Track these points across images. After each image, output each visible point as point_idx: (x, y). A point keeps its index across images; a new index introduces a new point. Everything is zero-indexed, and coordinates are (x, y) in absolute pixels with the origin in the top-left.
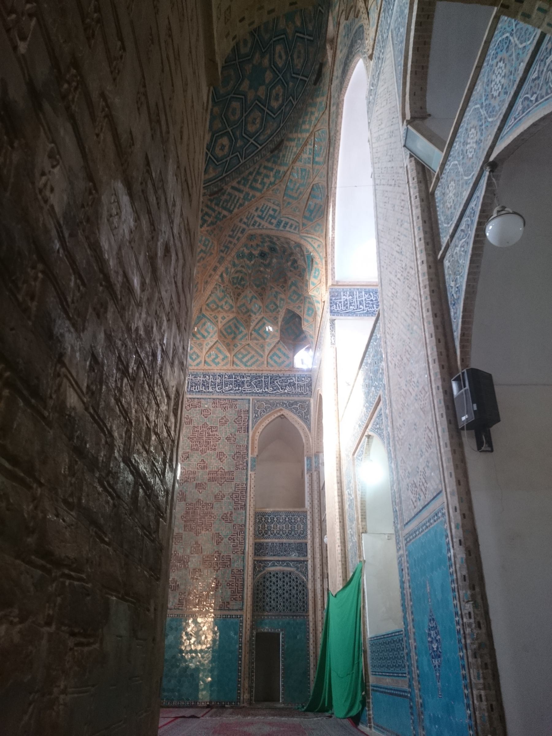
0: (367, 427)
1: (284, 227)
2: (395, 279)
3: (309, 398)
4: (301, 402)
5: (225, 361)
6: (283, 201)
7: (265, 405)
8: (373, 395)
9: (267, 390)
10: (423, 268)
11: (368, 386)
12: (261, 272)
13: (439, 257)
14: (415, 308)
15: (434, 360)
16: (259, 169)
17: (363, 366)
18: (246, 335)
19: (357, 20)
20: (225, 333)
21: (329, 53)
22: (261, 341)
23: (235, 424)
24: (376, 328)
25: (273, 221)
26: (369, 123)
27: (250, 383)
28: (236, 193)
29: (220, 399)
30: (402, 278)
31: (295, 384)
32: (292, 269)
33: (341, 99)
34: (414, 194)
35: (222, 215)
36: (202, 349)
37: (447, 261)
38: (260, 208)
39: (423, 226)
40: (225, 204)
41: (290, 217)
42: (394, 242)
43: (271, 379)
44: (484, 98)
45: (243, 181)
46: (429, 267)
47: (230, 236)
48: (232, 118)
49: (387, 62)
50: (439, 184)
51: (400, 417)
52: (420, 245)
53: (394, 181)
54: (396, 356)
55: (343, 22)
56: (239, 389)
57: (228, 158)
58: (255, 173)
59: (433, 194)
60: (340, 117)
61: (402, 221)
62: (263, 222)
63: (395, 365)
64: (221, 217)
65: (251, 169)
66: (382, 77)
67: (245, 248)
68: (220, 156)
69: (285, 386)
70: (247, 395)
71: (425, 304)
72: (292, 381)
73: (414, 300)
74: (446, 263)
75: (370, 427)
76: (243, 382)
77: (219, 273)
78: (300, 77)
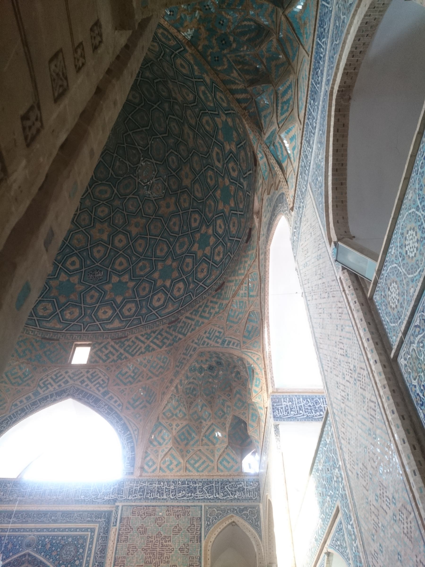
0: (325, 542)
1: (228, 344)
2: (344, 382)
3: (258, 504)
4: (251, 508)
5: (179, 467)
6: (226, 325)
7: (216, 512)
8: (329, 505)
9: (218, 496)
10: (377, 368)
11: (321, 495)
12: (210, 383)
13: (392, 355)
14: (375, 411)
15: (414, 472)
16: (207, 303)
17: (313, 473)
18: (197, 441)
19: (277, 191)
20: (178, 439)
21: (256, 221)
22: (212, 446)
23: (188, 533)
24: (324, 433)
25: (219, 340)
26: (295, 256)
27: (202, 489)
28: (189, 321)
29: (173, 506)
30: (352, 381)
31: (244, 489)
32: (236, 379)
33: (267, 249)
34: (352, 300)
35: (178, 338)
36: (158, 456)
37: (403, 359)
38: (208, 331)
39: (368, 327)
40: (181, 329)
41: (233, 337)
42: (336, 346)
43: (221, 484)
44: (419, 202)
45: (194, 313)
46: (384, 366)
47: (184, 354)
48: (186, 269)
49: (308, 206)
50: (377, 289)
51: (374, 540)
52: (369, 345)
53: (327, 294)
54: (358, 464)
55: (266, 197)
56: (191, 496)
57: (183, 297)
58: (203, 306)
59: (371, 298)
60: (267, 261)
61: (342, 326)
62: (210, 342)
63: (358, 474)
64: (177, 339)
66: (303, 219)
67: (196, 363)
68: (177, 296)
69: (235, 492)
70: (199, 502)
71: (388, 405)
72: (241, 486)
73: (372, 402)
74: (402, 361)
75: (328, 542)
76: (195, 488)
77: (175, 385)
78: (235, 239)
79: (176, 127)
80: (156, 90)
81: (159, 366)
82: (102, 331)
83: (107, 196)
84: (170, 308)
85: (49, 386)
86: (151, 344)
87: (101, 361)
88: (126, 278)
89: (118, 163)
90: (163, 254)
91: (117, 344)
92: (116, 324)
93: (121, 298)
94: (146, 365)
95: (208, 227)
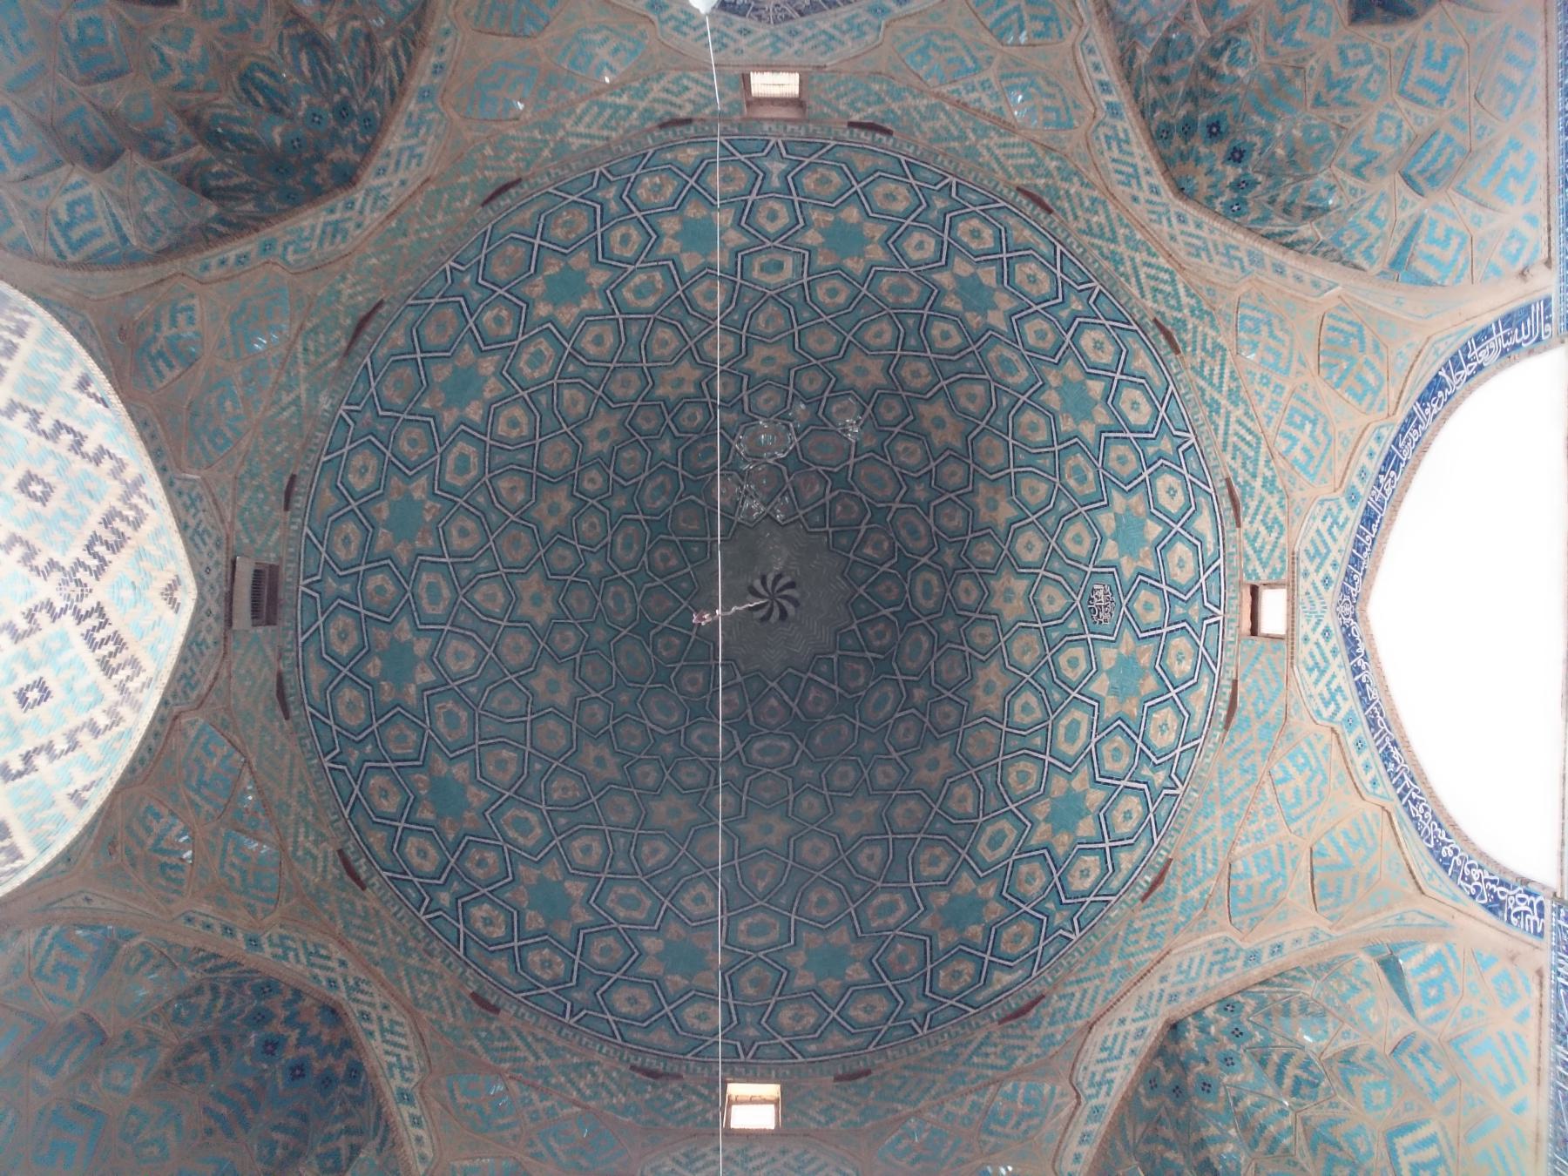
28: (1143, 276)
62: (1141, 165)
65: (1096, 252)
67: (1217, 202)
79: (764, 397)
80: (696, 437)
81: (1273, 343)
82: (1221, 561)
83: (935, 580)
84: (1142, 362)
85: (1333, 686)
86: (1225, 388)
87: (1283, 540)
88: (1106, 520)
89: (868, 551)
90: (1042, 421)
91: (1247, 508)
92: (1203, 524)
93: (1149, 522)
94: (1277, 386)
95: (942, 292)
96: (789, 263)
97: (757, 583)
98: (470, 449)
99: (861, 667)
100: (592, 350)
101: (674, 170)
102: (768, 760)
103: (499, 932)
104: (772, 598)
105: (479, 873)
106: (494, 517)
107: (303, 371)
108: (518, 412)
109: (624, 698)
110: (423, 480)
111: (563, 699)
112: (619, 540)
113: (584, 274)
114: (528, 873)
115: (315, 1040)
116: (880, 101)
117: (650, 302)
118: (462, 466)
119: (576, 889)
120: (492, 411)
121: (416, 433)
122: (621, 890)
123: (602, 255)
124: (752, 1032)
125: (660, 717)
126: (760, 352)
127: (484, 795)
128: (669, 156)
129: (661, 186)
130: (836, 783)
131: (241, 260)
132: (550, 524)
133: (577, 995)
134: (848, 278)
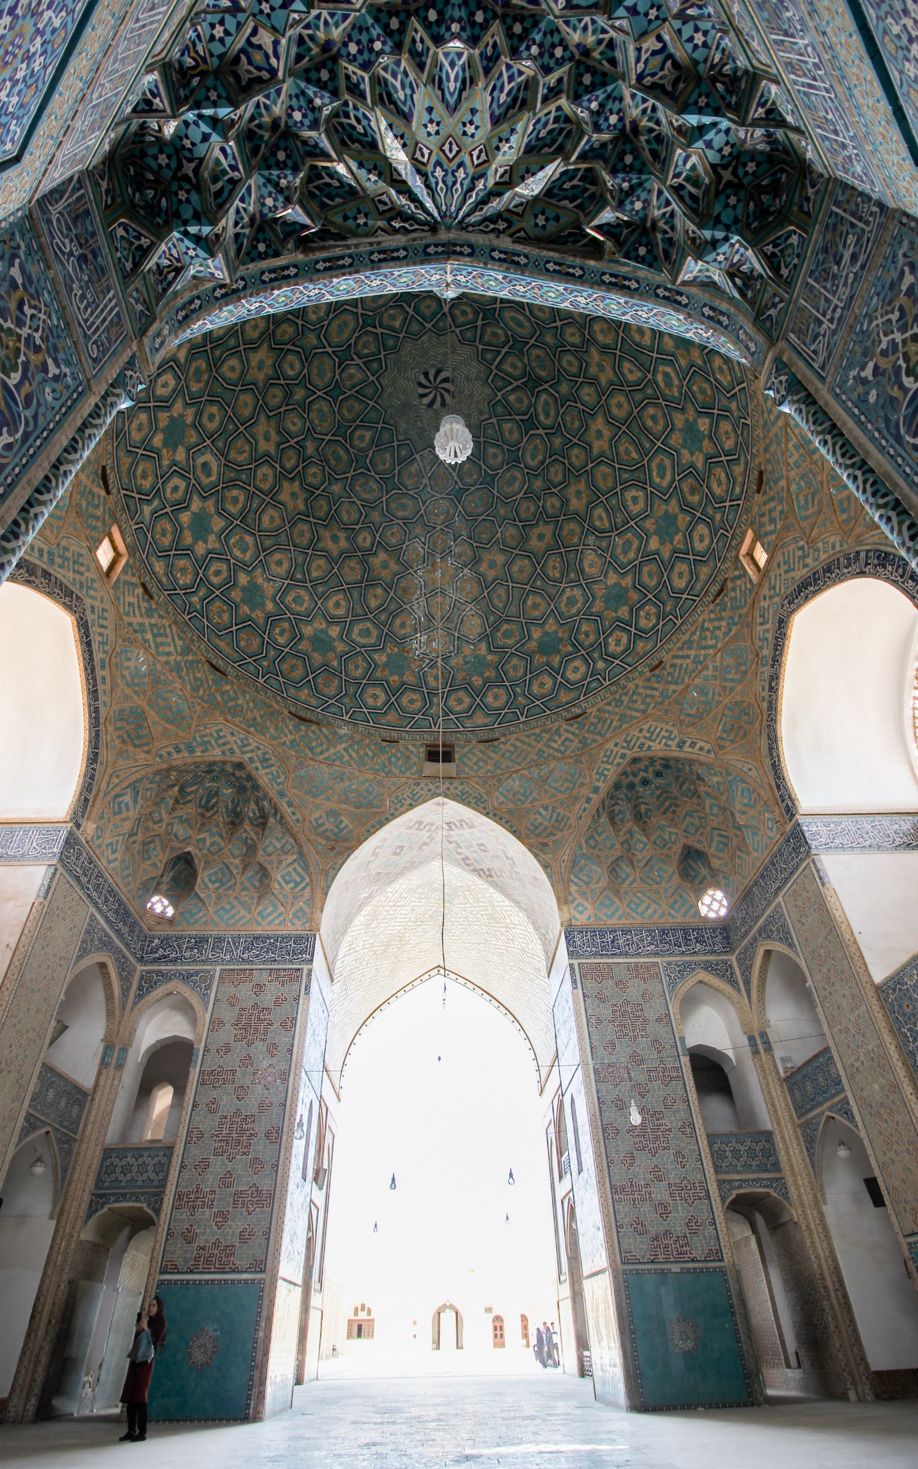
89: (397, 324)
96: (200, 460)
97: (426, 401)
98: (356, 630)
99: (489, 330)
100: (285, 566)
101: (169, 573)
102: (552, 413)
103: (625, 639)
104: (436, 388)
105: (592, 638)
106: (393, 607)
107: (332, 751)
108: (331, 603)
109: (502, 512)
110: (376, 656)
111: (500, 558)
112: (400, 514)
113: (244, 589)
114: (598, 606)
115: (647, 767)
116: (91, 492)
117: (249, 539)
118: (366, 633)
119: (612, 578)
120: (332, 620)
121: (351, 667)
122: (619, 550)
123: (230, 583)
124: (718, 516)
125: (517, 485)
126: (264, 446)
127: (551, 621)
128: (164, 579)
129: (181, 570)
130: (574, 370)
131: (290, 804)
132: (394, 567)
133: (668, 609)
134: (199, 414)
